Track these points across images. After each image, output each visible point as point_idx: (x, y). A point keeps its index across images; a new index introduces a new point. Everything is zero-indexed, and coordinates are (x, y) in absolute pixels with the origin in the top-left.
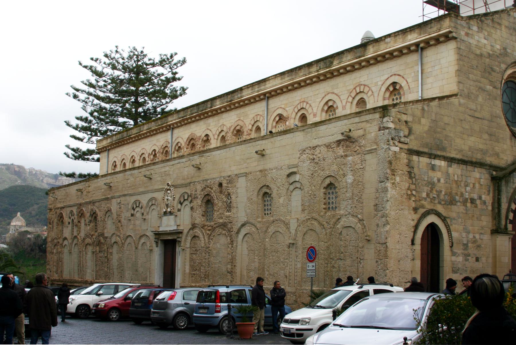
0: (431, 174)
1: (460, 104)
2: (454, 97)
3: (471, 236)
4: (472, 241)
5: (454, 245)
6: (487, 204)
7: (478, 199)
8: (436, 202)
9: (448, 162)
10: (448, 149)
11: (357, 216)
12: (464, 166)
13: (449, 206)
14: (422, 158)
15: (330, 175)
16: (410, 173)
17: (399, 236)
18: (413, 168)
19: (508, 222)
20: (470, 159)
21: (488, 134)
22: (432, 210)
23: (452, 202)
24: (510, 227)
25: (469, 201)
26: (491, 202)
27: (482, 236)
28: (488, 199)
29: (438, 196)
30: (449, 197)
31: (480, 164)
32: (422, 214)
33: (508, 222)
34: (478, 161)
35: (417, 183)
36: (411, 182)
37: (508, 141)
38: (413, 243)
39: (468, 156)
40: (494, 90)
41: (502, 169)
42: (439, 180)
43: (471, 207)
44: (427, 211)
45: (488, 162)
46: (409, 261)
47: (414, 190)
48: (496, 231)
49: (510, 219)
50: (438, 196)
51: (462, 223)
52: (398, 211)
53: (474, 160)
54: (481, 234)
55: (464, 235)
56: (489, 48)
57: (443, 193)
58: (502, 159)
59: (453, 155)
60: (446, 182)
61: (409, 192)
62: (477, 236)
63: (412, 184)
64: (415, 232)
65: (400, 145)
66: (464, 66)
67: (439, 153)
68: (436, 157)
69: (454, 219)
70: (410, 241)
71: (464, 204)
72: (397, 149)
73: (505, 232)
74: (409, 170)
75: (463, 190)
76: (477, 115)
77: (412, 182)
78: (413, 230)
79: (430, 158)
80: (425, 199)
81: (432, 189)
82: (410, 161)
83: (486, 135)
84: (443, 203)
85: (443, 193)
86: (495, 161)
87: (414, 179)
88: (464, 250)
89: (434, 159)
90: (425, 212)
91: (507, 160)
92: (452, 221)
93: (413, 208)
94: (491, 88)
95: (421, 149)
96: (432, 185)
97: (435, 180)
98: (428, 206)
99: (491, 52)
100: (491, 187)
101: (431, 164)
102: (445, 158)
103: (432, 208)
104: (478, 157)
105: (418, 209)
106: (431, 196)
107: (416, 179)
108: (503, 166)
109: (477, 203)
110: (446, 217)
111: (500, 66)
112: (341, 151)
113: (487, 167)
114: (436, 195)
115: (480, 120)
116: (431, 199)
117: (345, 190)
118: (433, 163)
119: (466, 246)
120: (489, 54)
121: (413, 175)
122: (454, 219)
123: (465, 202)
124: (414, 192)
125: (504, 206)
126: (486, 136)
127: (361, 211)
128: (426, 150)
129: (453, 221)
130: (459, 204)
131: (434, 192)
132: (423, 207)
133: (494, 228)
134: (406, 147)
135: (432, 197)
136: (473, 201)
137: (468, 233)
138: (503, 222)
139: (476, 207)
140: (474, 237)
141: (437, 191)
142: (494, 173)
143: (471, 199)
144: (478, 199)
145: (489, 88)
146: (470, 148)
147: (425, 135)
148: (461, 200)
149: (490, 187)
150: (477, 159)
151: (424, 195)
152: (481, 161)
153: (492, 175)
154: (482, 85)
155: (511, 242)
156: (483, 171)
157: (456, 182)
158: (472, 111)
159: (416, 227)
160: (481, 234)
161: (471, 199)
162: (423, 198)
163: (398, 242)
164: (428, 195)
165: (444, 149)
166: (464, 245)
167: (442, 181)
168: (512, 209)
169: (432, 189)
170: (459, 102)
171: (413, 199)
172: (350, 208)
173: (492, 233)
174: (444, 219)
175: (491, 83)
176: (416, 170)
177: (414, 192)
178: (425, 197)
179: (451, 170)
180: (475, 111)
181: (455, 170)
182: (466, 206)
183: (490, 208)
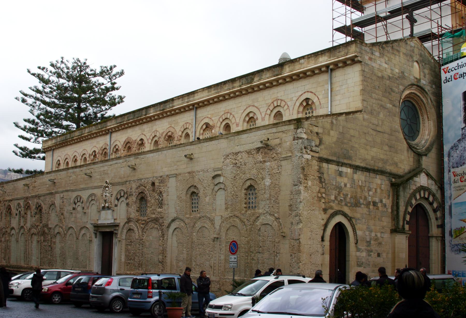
0: (339, 179)
1: (364, 119)
2: (359, 113)
3: (373, 234)
5: (359, 242)
6: (387, 207)
8: (343, 204)
9: (353, 169)
10: (353, 158)
11: (273, 215)
12: (368, 174)
13: (354, 208)
14: (331, 165)
15: (250, 178)
16: (320, 178)
17: (310, 233)
18: (323, 174)
19: (405, 223)
20: (372, 167)
21: (388, 146)
22: (340, 211)
23: (357, 204)
24: (407, 227)
25: (372, 203)
26: (390, 205)
27: (383, 234)
28: (388, 202)
29: (345, 199)
30: (354, 200)
31: (381, 172)
32: (331, 214)
33: (405, 223)
34: (379, 169)
35: (326, 187)
36: (321, 186)
37: (406, 153)
38: (323, 240)
39: (371, 164)
40: (394, 108)
41: (400, 177)
42: (345, 185)
43: (373, 209)
44: (335, 212)
45: (388, 170)
46: (320, 255)
47: (324, 193)
48: (395, 230)
49: (407, 221)
50: (345, 199)
51: (365, 223)
52: (309, 211)
53: (376, 168)
54: (382, 232)
55: (367, 233)
56: (389, 71)
57: (349, 196)
58: (401, 168)
59: (357, 164)
60: (352, 187)
61: (320, 195)
62: (379, 235)
63: (322, 187)
64: (324, 230)
65: (312, 153)
66: (367, 86)
67: (346, 161)
68: (343, 165)
69: (359, 219)
70: (320, 237)
71: (367, 206)
72: (309, 157)
73: (402, 231)
74: (319, 176)
75: (367, 194)
76: (379, 129)
77: (322, 186)
78: (323, 228)
79: (338, 165)
80: (334, 201)
81: (339, 193)
82: (320, 167)
83: (387, 146)
84: (349, 205)
85: (349, 196)
86: (393, 169)
87: (324, 184)
88: (367, 246)
89: (342, 166)
90: (333, 213)
91: (404, 169)
93: (323, 209)
94: (391, 106)
95: (330, 158)
96: (339, 189)
97: (342, 185)
98: (336, 207)
99: (391, 75)
101: (339, 170)
102: (351, 166)
103: (340, 209)
104: (380, 165)
105: (328, 210)
106: (339, 198)
107: (325, 184)
108: (401, 174)
109: (379, 205)
110: (352, 218)
111: (399, 87)
112: (260, 157)
113: (387, 175)
114: (343, 197)
115: (381, 134)
116: (339, 201)
117: (263, 192)
118: (340, 170)
119: (369, 243)
120: (389, 76)
121: (323, 180)
122: (359, 219)
123: (368, 204)
124: (324, 195)
125: (402, 209)
126: (386, 148)
127: (277, 210)
128: (334, 159)
129: (358, 221)
130: (363, 206)
131: (342, 196)
132: (331, 208)
133: (393, 228)
134: (317, 155)
135: (339, 200)
136: (375, 204)
137: (371, 231)
138: (401, 223)
139: (378, 209)
140: (376, 235)
141: (343, 195)
142: (393, 180)
143: (373, 202)
145: (389, 106)
146: (373, 157)
147: (333, 145)
148: (365, 203)
149: (390, 192)
150: (378, 167)
151: (333, 197)
152: (382, 169)
153: (391, 181)
154: (383, 103)
155: (407, 240)
156: (384, 177)
157: (361, 187)
158: (375, 126)
159: (326, 226)
160: (382, 232)
161: (373, 202)
162: (332, 200)
163: (310, 238)
164: (336, 198)
165: (350, 158)
166: (367, 242)
167: (348, 185)
168: (408, 211)
169: (339, 193)
170: (363, 117)
171: (323, 201)
172: (268, 207)
173: (391, 232)
174: (350, 219)
175: (391, 102)
176: (325, 176)
177: (324, 195)
178: (334, 199)
179: (356, 177)
180: (377, 126)
181: (360, 177)
182: (369, 209)
183: (390, 210)
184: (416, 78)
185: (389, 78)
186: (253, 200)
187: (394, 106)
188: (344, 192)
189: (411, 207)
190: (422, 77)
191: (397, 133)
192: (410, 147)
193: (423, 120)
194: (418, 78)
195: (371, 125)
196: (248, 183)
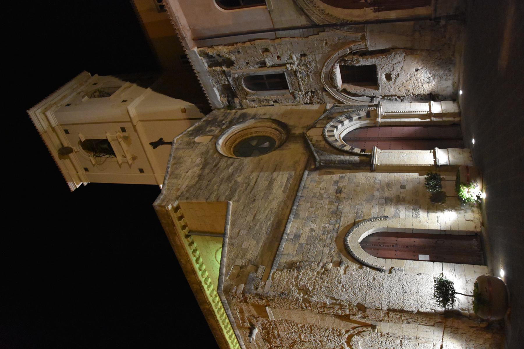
0: (303, 240)
4: (383, 192)
7: (337, 185)
21: (274, 172)
25: (338, 195)
30: (332, 218)
40: (234, 165)
42: (312, 230)
56: (195, 169)
58: (300, 158)
69: (357, 213)
81: (321, 240)
83: (274, 173)
92: (359, 216)
94: (231, 167)
99: (201, 166)
100: (326, 170)
111: (215, 158)
120: (201, 168)
130: (340, 207)
143: (337, 193)
144: (337, 185)
145: (230, 170)
146: (284, 192)
148: (336, 204)
149: (326, 172)
154: (226, 176)
169: (321, 240)
175: (228, 167)
180: (249, 185)
184: (211, 140)
185: (203, 168)
187: (232, 164)
188: (321, 232)
189: (345, 146)
190: (212, 133)
191: (262, 161)
192: (281, 146)
194: (211, 137)
195: (246, 192)
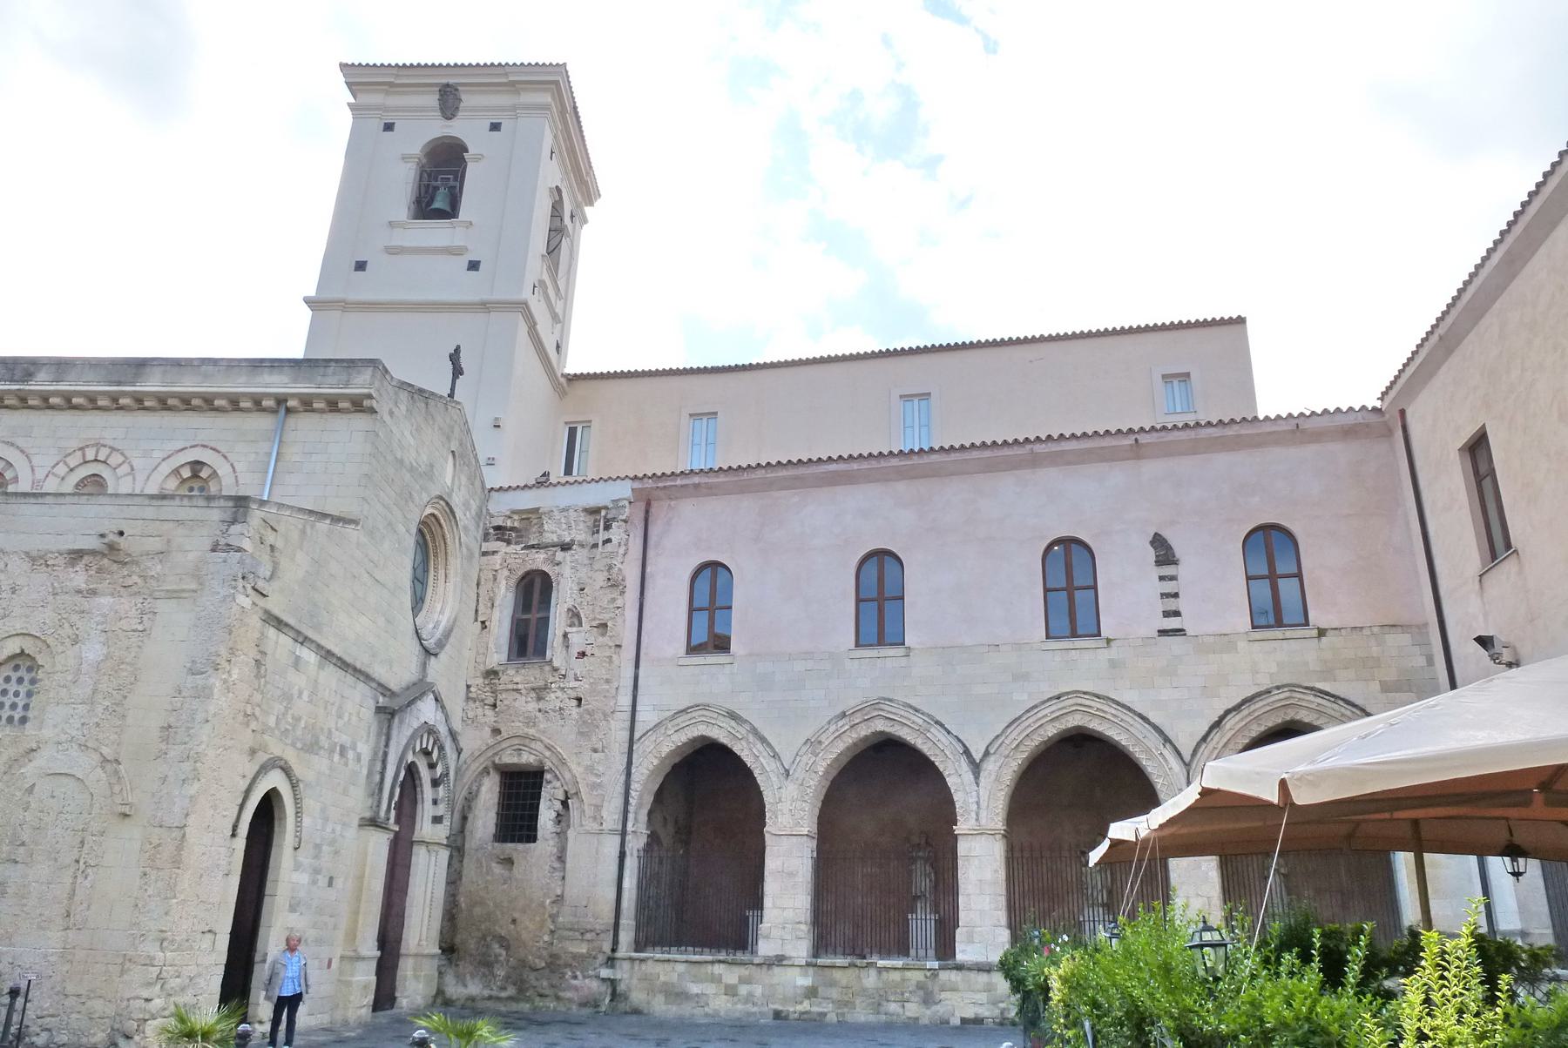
23: (312, 747)
25: (338, 748)
46: (219, 878)
52: (221, 750)
54: (344, 824)
57: (303, 724)
85: (303, 724)
97: (295, 691)
98: (276, 749)
101: (294, 653)
106: (283, 726)
112: (79, 577)
113: (374, 685)
124: (257, 711)
135: (283, 729)
139: (346, 764)
142: (381, 699)
151: (272, 721)
161: (341, 746)
165: (317, 627)
178: (273, 725)
186: (16, 700)
193: (436, 578)
196: (12, 647)
